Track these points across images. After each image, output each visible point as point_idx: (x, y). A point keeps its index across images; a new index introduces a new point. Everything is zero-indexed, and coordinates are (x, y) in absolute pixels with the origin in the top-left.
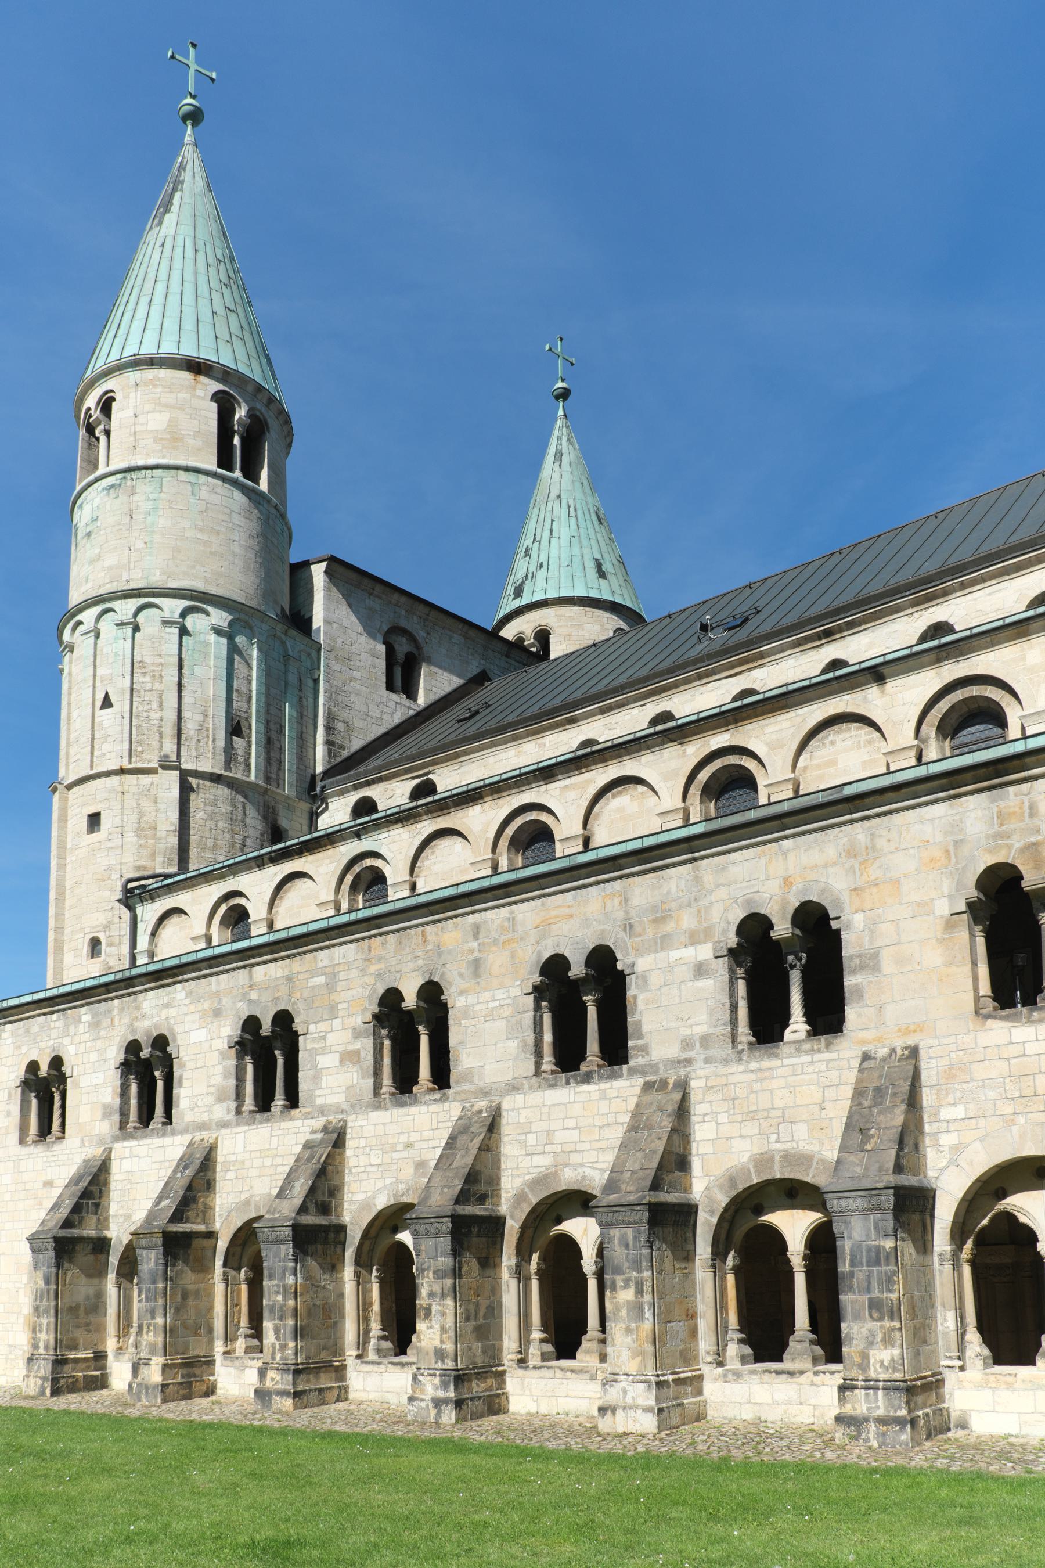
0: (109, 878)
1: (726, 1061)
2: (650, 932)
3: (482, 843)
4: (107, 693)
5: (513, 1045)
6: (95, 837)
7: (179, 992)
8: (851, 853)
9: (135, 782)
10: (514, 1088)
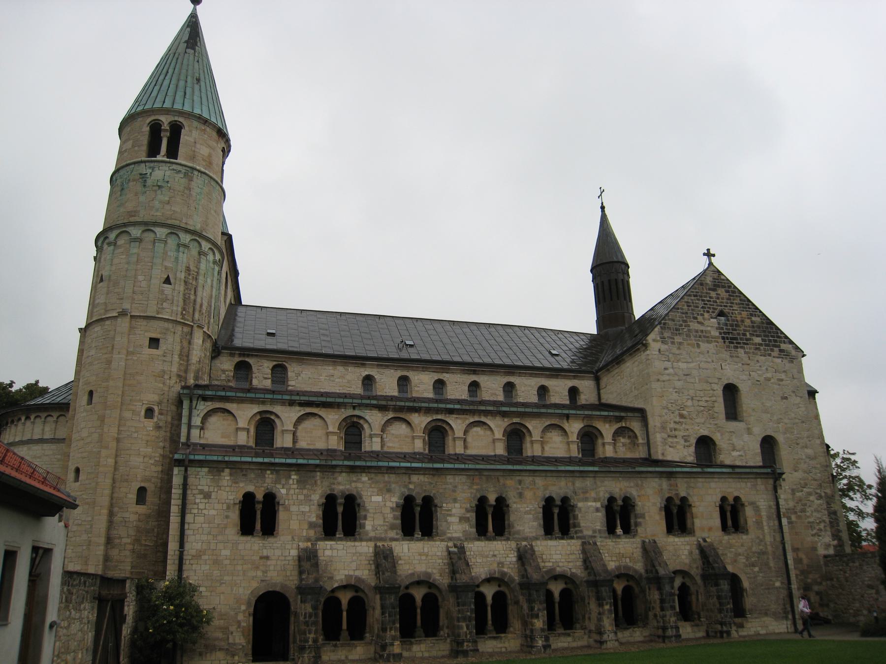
0: (162, 377)
1: (606, 538)
2: (582, 496)
3: (419, 429)
4: (168, 276)
5: (535, 524)
6: (154, 351)
7: (365, 478)
8: (637, 485)
9: (181, 329)
10: (536, 538)
